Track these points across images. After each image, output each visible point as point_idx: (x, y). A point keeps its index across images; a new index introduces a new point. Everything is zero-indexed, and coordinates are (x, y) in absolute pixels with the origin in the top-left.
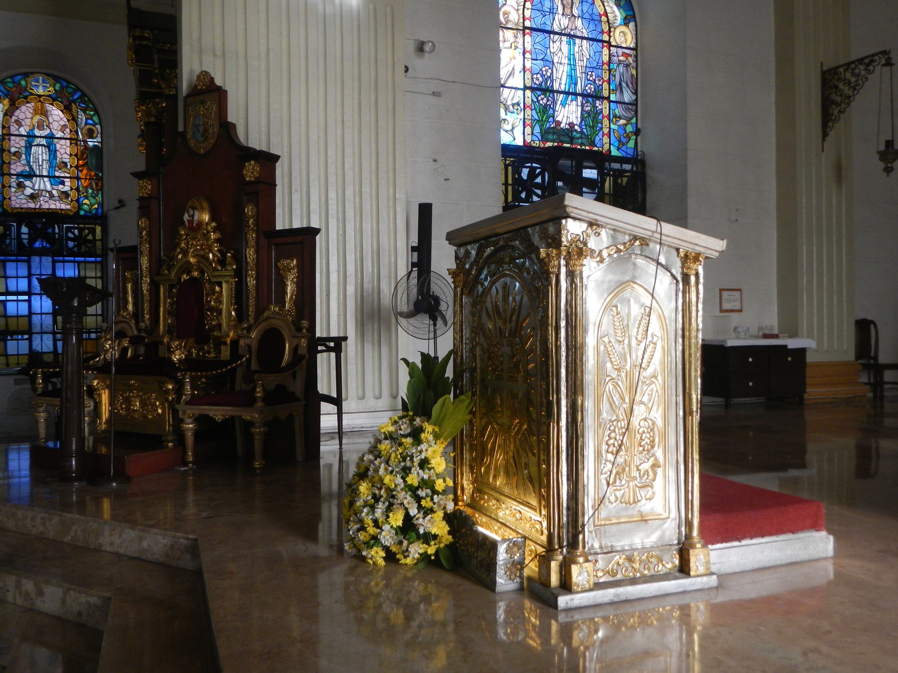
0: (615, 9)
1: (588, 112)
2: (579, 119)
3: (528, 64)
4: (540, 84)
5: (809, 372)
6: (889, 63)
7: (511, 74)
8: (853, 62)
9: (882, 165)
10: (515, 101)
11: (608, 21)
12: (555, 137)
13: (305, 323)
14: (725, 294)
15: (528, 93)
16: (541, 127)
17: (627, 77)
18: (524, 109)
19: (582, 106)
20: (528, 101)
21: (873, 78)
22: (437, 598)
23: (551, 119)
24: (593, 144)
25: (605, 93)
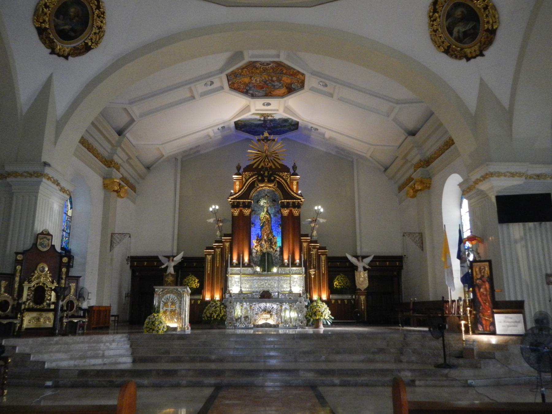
6: (130, 237)
8: (120, 234)
9: (127, 262)
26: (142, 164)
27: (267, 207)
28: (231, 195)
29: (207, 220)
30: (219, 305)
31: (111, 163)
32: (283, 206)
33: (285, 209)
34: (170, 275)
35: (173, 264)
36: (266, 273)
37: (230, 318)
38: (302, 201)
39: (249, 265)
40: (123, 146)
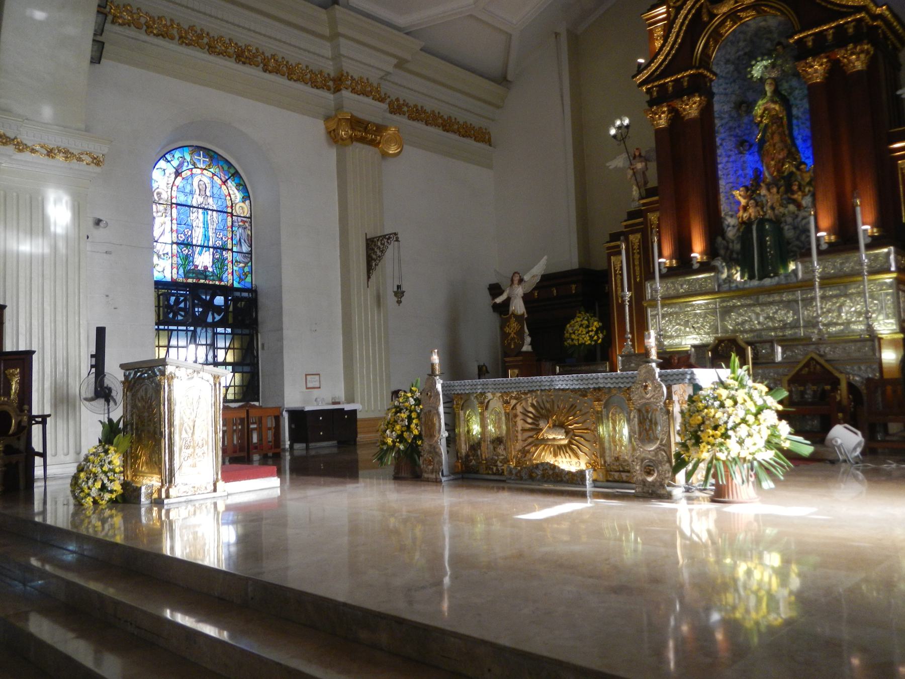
0: (236, 191)
1: (217, 259)
2: (211, 264)
3: (175, 227)
4: (184, 241)
5: (358, 423)
6: (397, 240)
7: (163, 233)
8: (381, 236)
9: (396, 299)
10: (165, 252)
11: (231, 199)
12: (194, 275)
13: (26, 407)
14: (309, 377)
15: (175, 246)
16: (184, 269)
17: (245, 236)
18: (172, 257)
19: (213, 255)
20: (175, 252)
21: (390, 247)
22: (116, 516)
23: (191, 263)
24: (221, 280)
25: (229, 246)
26: (481, 75)
27: (776, 82)
28: (640, 69)
29: (607, 164)
30: (412, 401)
31: (340, 80)
32: (802, 52)
33: (810, 59)
34: (513, 319)
35: (519, 291)
36: (755, 283)
37: (431, 445)
38: (875, 17)
39: (705, 267)
40: (341, 29)
